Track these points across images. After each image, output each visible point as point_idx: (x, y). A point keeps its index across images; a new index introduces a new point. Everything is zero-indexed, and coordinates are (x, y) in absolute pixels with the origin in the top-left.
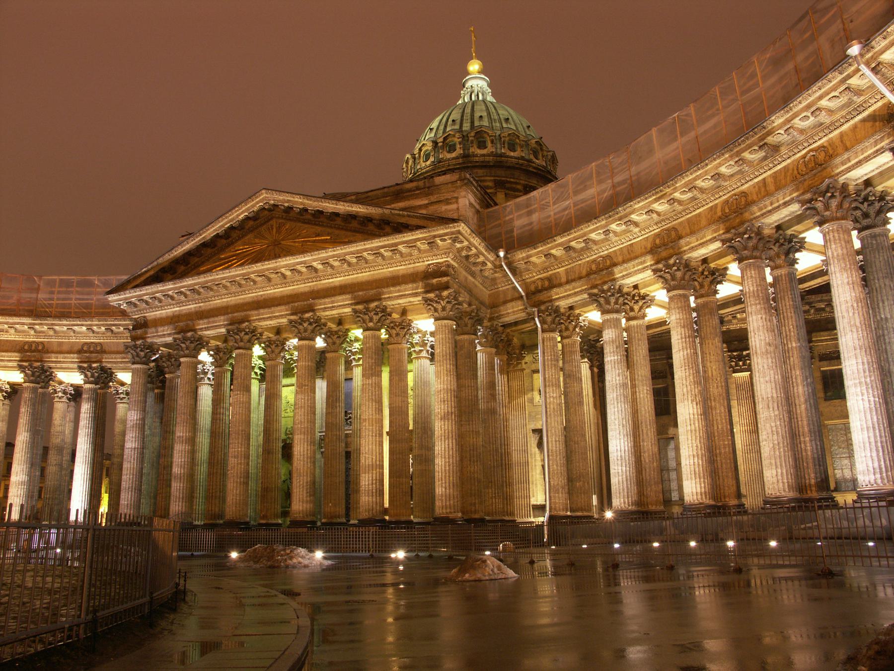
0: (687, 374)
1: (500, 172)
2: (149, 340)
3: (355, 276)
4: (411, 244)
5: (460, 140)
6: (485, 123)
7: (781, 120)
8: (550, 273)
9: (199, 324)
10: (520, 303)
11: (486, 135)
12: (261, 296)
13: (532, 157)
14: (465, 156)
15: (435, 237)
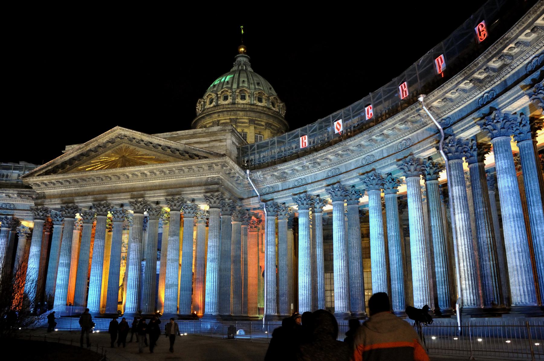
0: (340, 245)
1: (252, 114)
2: (46, 206)
3: (168, 180)
4: (199, 167)
5: (231, 94)
6: (246, 85)
7: (390, 124)
8: (273, 184)
9: (76, 199)
10: (256, 198)
11: (245, 92)
12: (114, 186)
13: (271, 106)
14: (234, 103)
15: (212, 163)
